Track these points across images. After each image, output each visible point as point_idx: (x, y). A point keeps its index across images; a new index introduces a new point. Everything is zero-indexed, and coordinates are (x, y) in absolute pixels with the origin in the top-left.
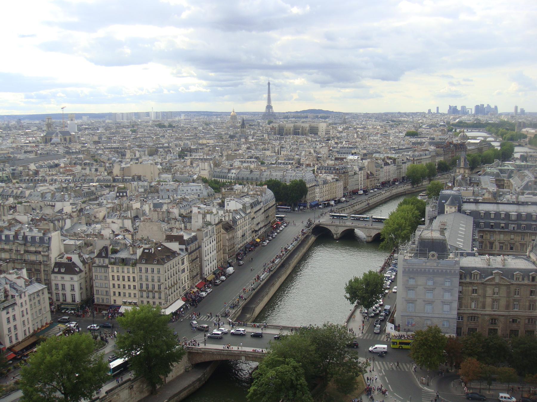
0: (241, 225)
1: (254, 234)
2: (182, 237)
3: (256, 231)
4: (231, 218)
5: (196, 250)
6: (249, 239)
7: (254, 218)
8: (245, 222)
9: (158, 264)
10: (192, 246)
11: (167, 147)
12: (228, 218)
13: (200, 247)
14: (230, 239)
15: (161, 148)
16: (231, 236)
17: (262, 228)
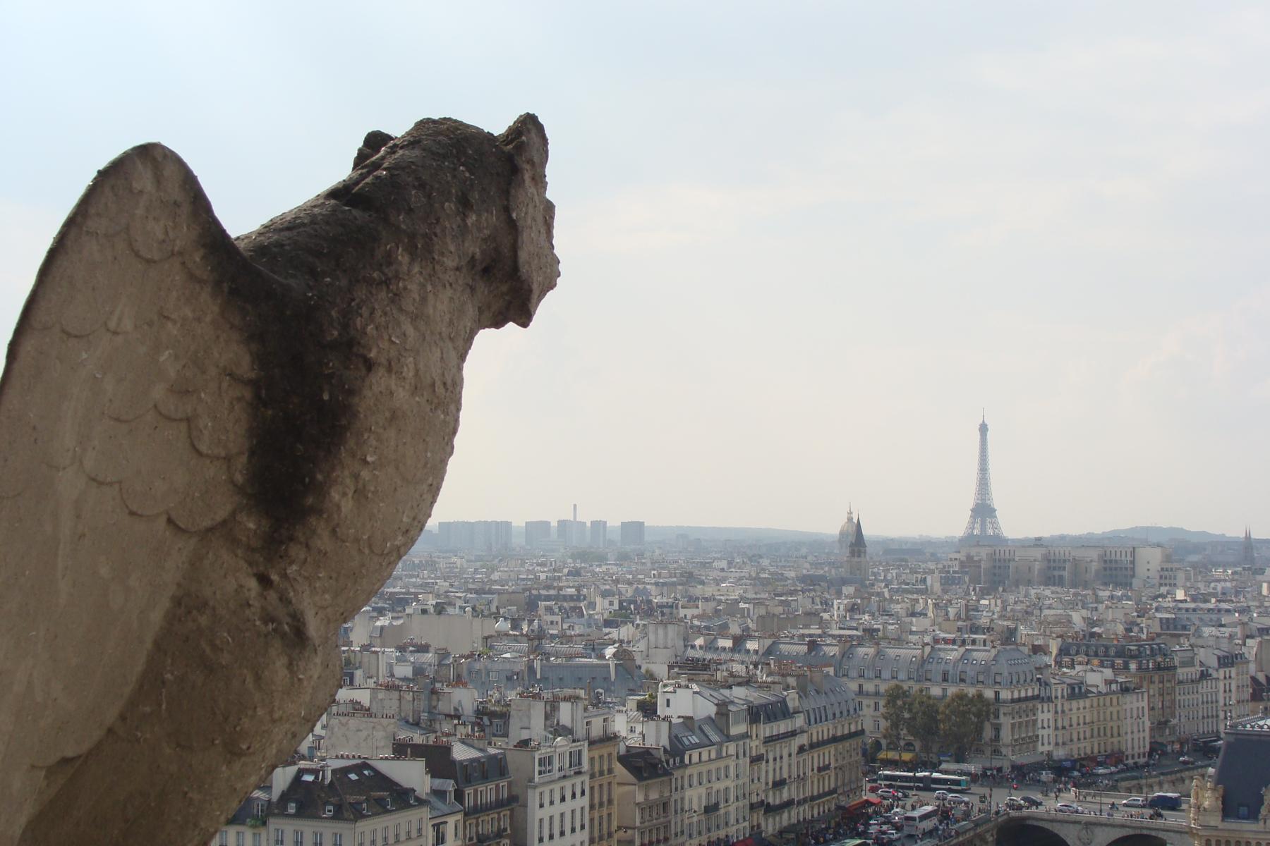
0: (704, 769)
1: (759, 818)
2: (447, 750)
3: (770, 809)
4: (664, 741)
5: (499, 804)
6: (737, 829)
7: (756, 760)
8: (722, 764)
9: (338, 816)
10: (487, 792)
11: (571, 598)
12: (652, 736)
13: (513, 802)
14: (647, 807)
15: (548, 598)
16: (654, 796)
17: (799, 803)
